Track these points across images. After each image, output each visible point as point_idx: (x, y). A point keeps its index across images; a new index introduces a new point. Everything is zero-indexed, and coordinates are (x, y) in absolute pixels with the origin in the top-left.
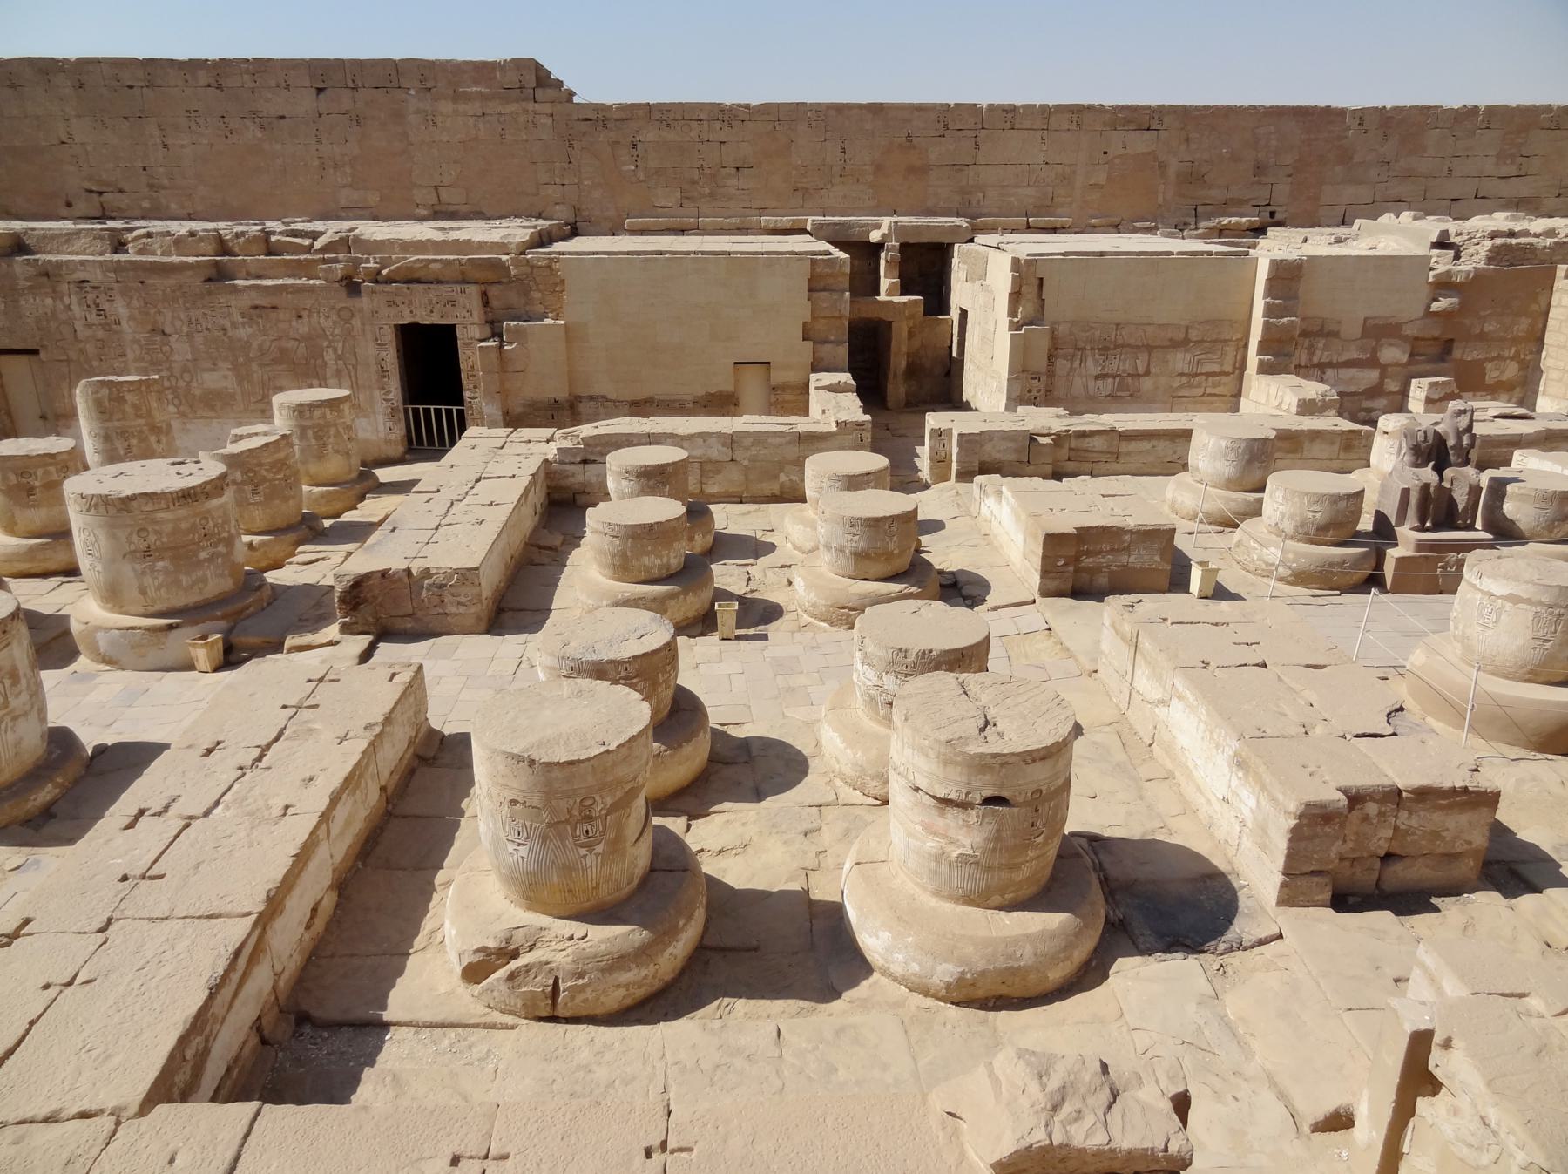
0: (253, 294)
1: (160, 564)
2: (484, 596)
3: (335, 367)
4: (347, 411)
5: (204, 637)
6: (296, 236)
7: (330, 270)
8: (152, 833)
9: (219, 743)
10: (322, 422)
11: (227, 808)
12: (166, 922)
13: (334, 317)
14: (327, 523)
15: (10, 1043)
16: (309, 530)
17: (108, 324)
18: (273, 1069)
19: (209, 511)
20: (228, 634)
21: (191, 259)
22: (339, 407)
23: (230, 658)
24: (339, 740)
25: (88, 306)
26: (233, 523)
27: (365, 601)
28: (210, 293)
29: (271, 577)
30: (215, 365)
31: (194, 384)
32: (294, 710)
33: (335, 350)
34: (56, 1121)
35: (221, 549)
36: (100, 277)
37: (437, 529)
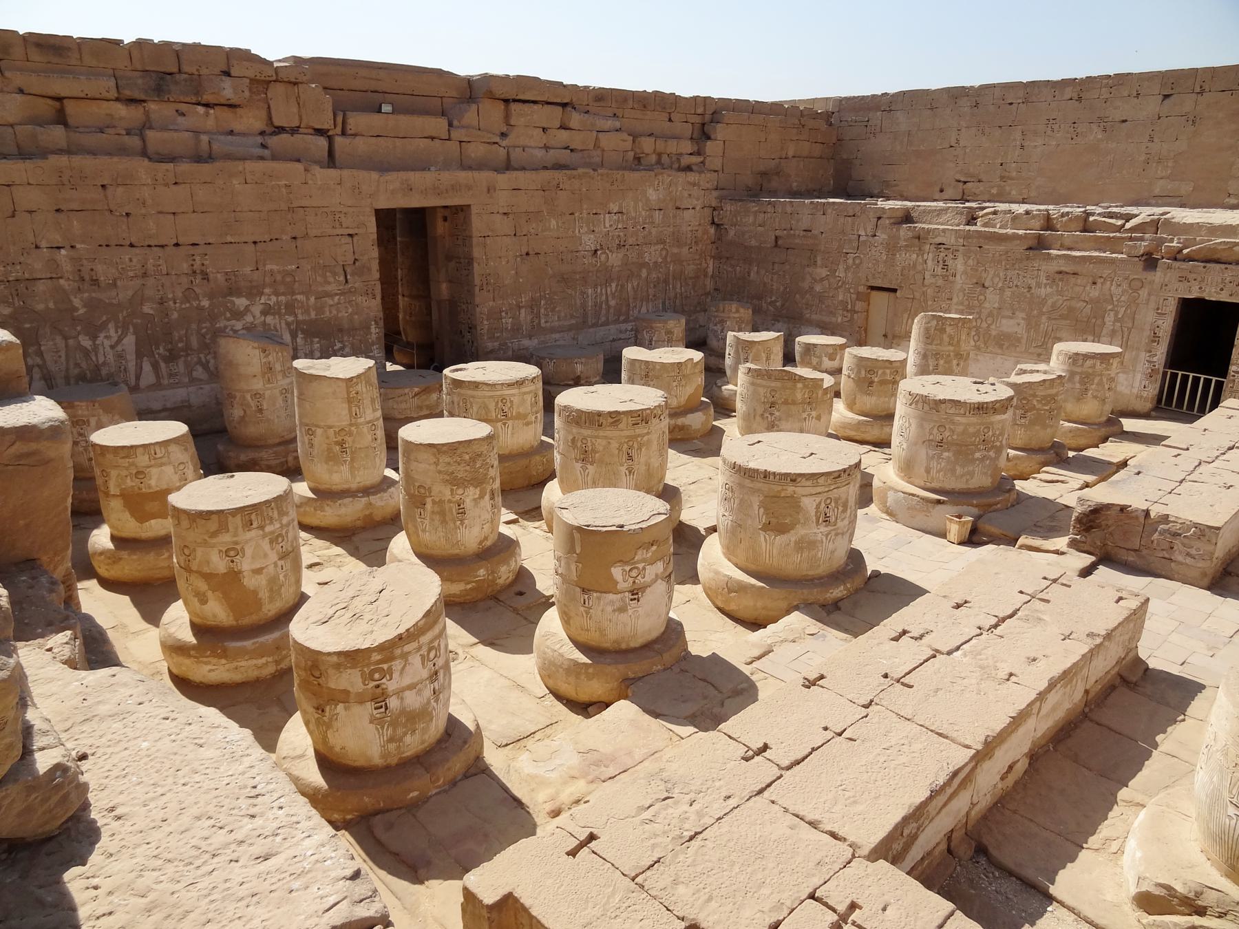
0: (1062, 262)
1: (946, 454)
2: (1216, 555)
3: (1112, 328)
4: (1115, 365)
5: (960, 517)
6: (1112, 218)
7: (1135, 247)
8: (909, 653)
9: (966, 602)
10: (1090, 371)
11: (965, 655)
12: (908, 722)
13: (1125, 286)
14: (1071, 454)
15: (799, 756)
16: (1056, 455)
17: (947, 276)
18: (951, 876)
19: (992, 423)
20: (978, 518)
21: (1021, 232)
22: (1109, 360)
23: (973, 539)
24: (1063, 637)
26: (1006, 436)
27: (1099, 526)
28: (1028, 258)
29: (1019, 485)
30: (1013, 314)
31: (993, 327)
32: (1029, 598)
33: (1116, 315)
34: (816, 828)
35: (992, 454)
36: (953, 241)
37: (1181, 482)
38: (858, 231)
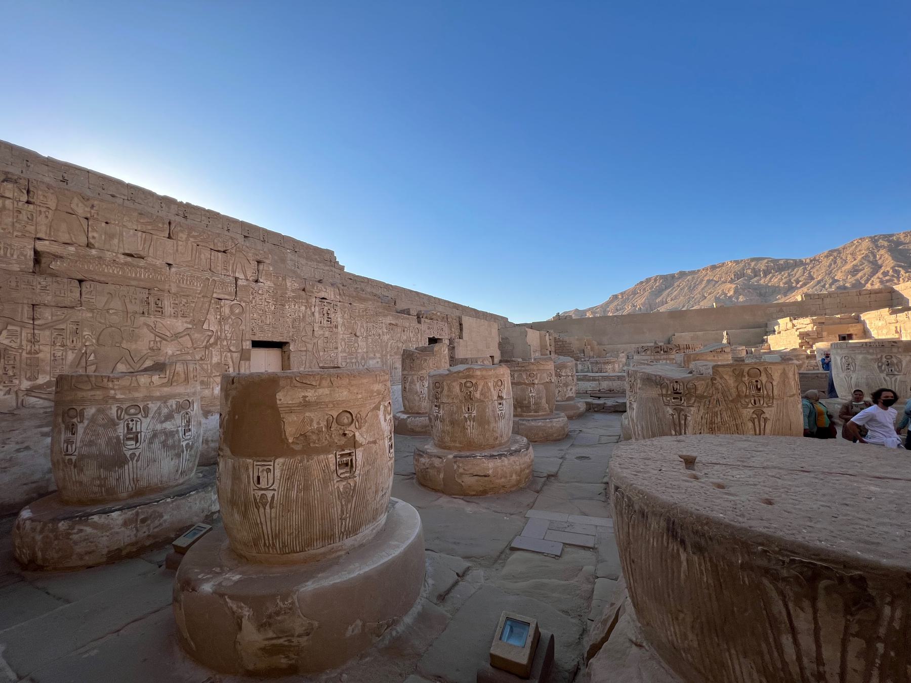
25: (324, 315)
38: (234, 272)
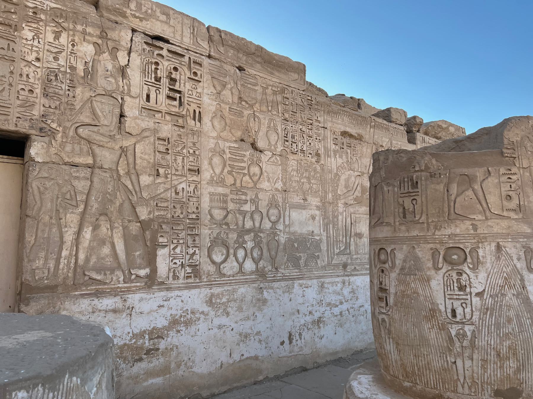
17: (182, 116)
25: (158, 79)
36: (187, 41)
